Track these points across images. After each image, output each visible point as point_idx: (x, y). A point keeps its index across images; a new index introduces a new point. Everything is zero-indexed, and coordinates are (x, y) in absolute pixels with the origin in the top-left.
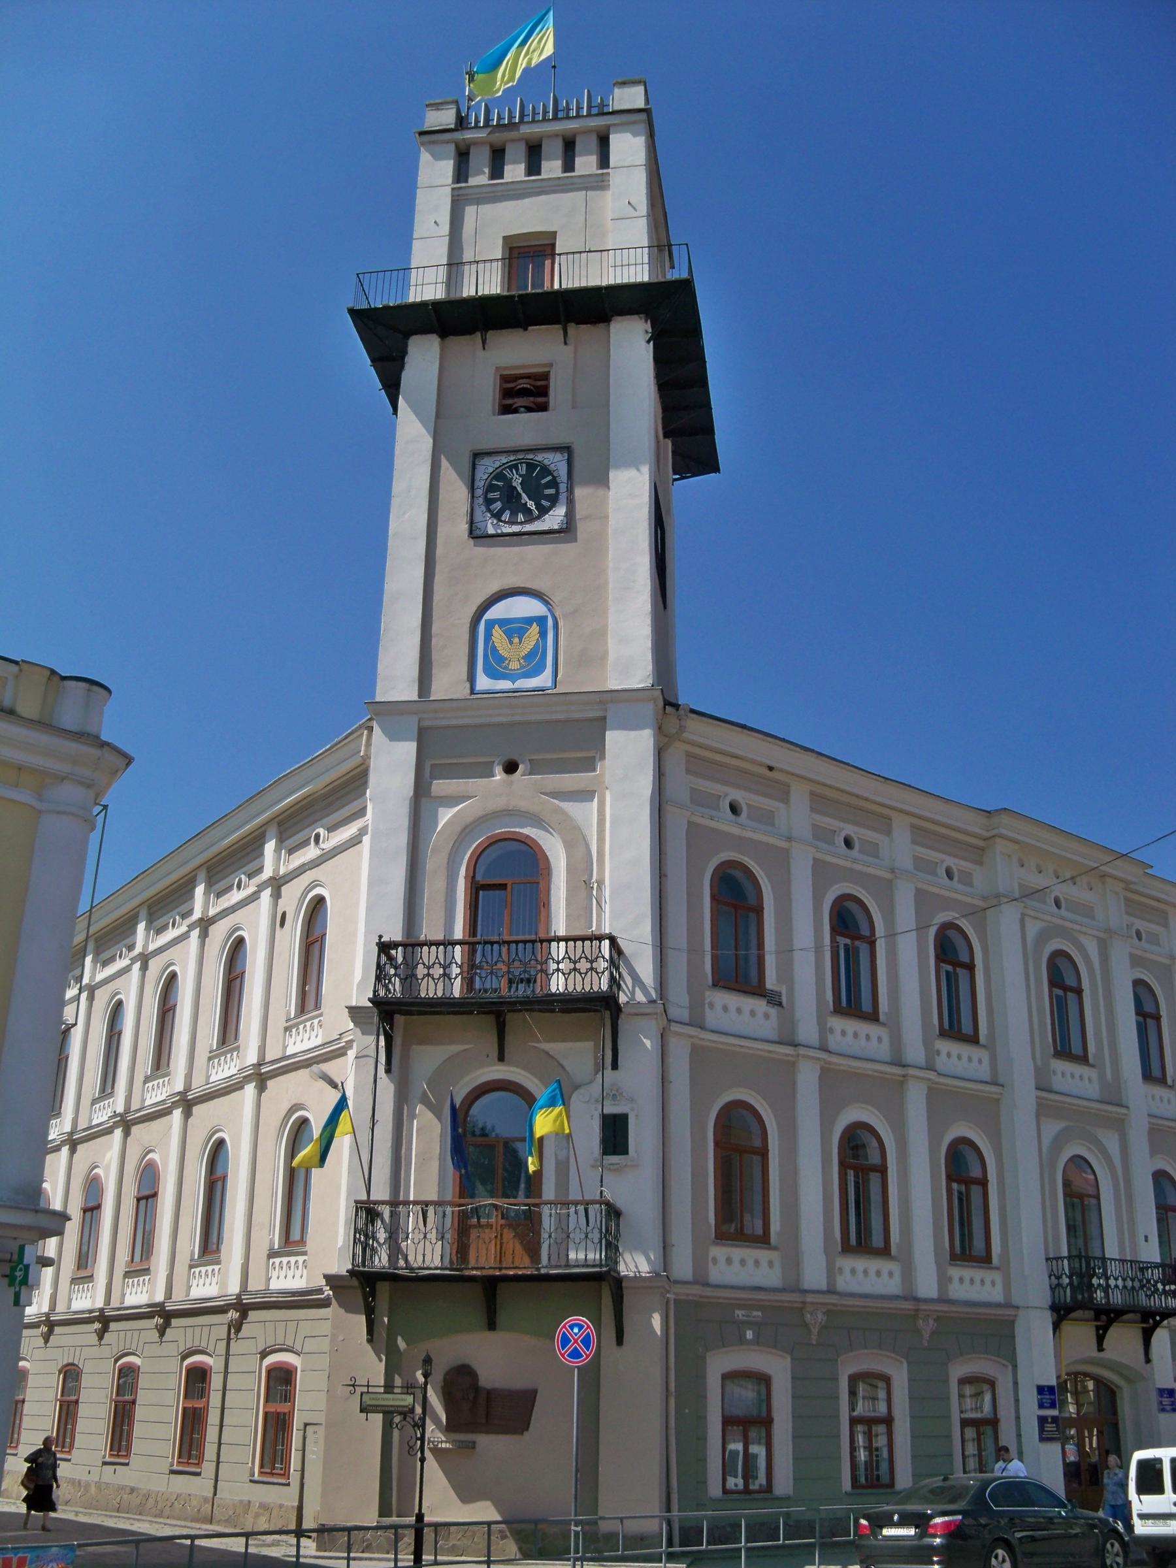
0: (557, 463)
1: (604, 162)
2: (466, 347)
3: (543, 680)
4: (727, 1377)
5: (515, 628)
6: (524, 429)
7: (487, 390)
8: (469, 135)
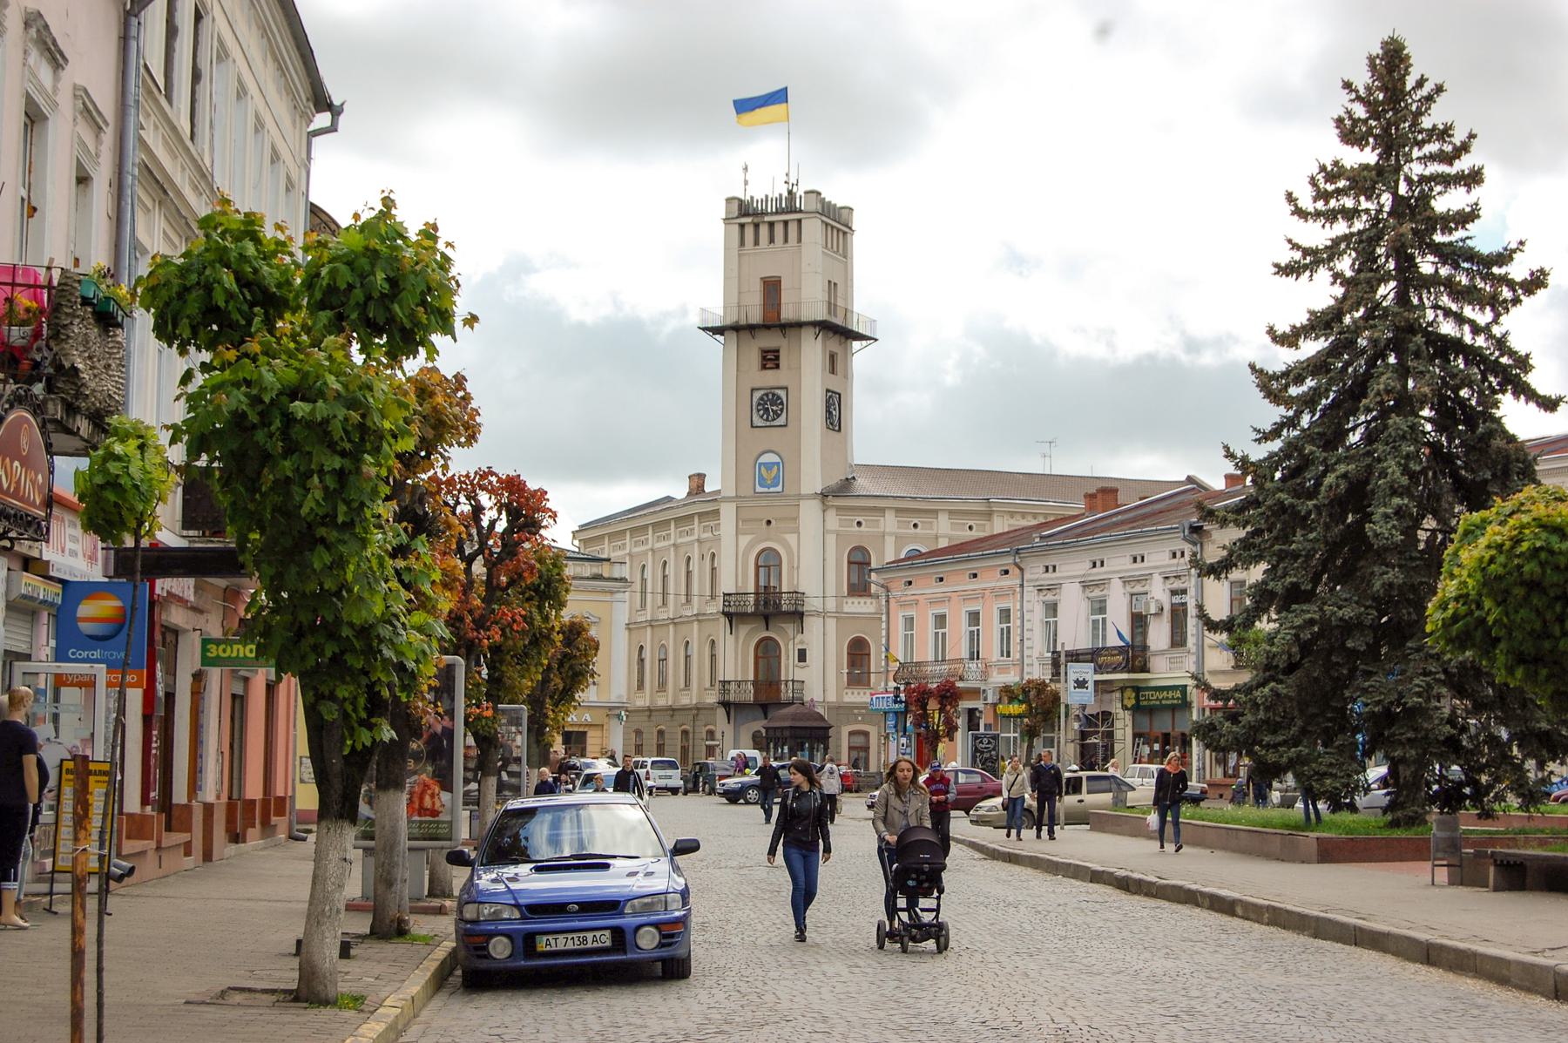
0: (782, 393)
1: (800, 240)
2: (745, 335)
3: (779, 489)
4: (851, 733)
5: (769, 466)
6: (770, 378)
7: (754, 358)
8: (743, 220)
